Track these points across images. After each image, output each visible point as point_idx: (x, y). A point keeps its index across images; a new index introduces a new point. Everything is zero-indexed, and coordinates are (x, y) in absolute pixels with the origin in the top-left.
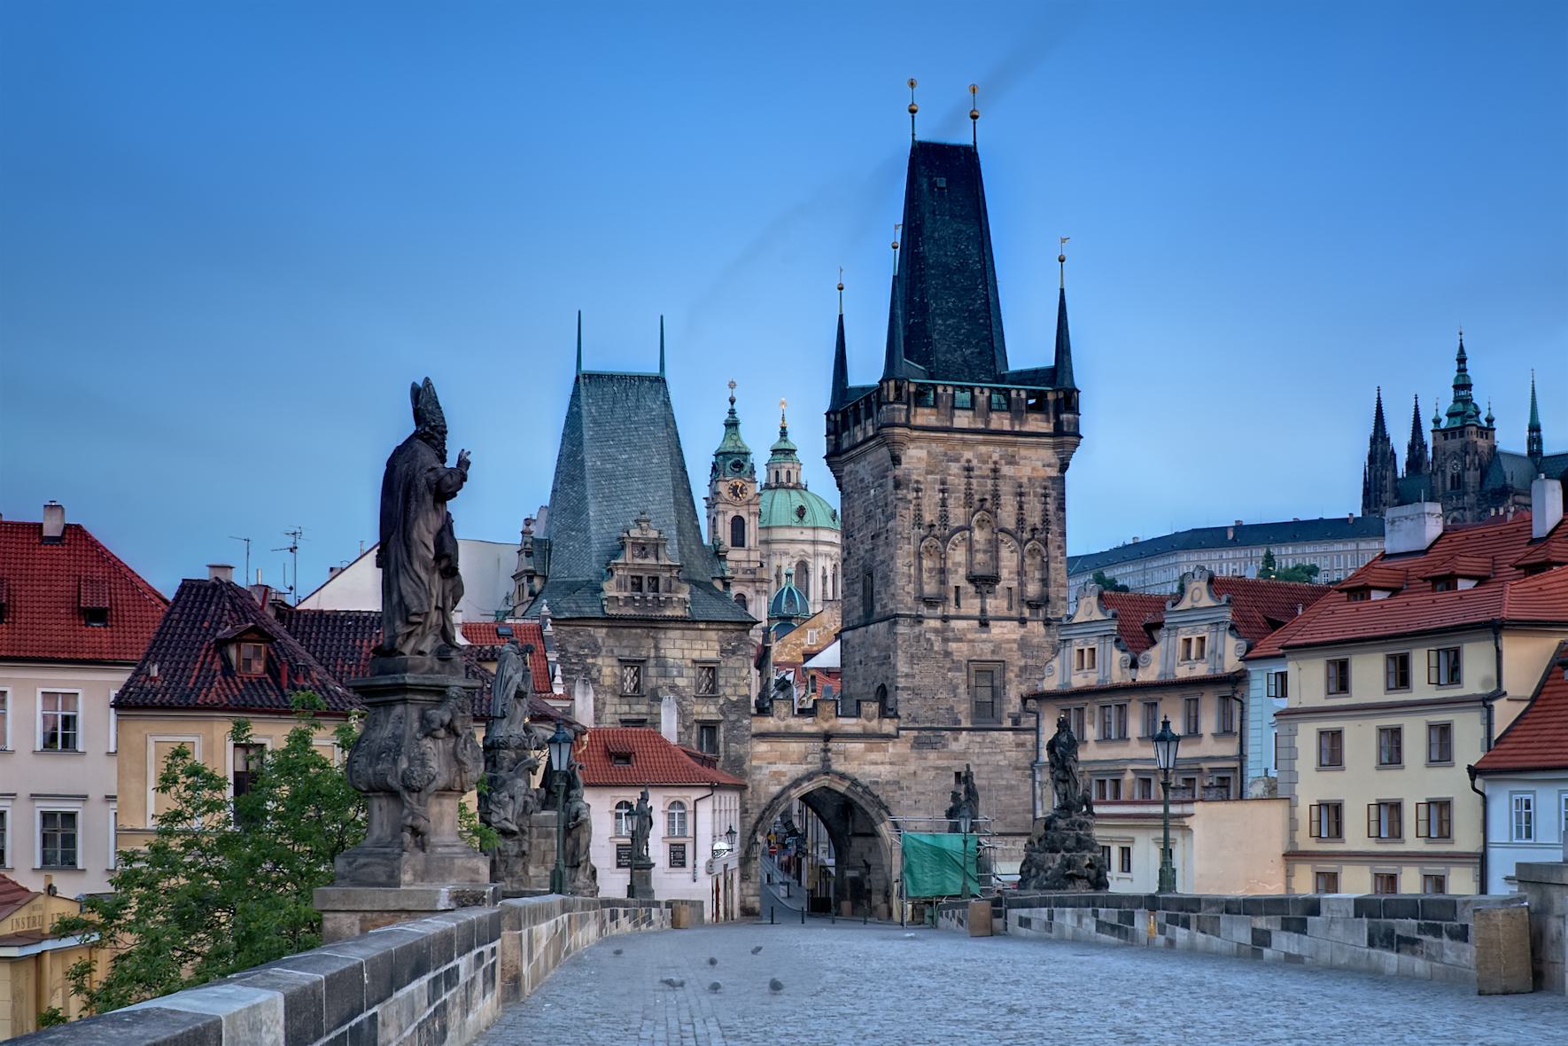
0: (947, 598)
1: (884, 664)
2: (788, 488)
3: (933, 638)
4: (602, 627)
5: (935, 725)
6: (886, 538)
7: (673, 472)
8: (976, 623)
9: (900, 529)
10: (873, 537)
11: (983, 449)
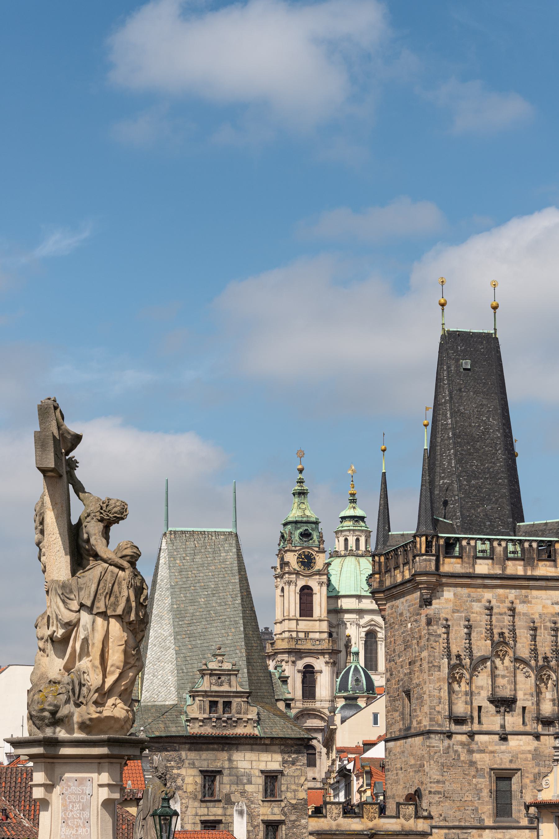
0: (472, 718)
1: (419, 771)
2: (358, 556)
3: (460, 750)
4: (185, 743)
5: (462, 824)
6: (421, 665)
7: (244, 612)
8: (497, 737)
9: (431, 659)
10: (410, 663)
11: (501, 591)
